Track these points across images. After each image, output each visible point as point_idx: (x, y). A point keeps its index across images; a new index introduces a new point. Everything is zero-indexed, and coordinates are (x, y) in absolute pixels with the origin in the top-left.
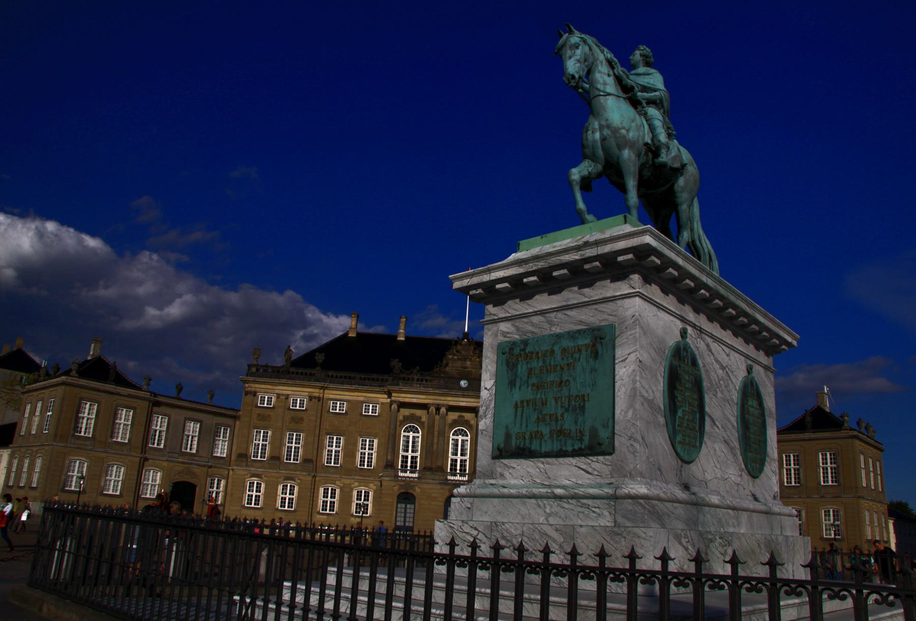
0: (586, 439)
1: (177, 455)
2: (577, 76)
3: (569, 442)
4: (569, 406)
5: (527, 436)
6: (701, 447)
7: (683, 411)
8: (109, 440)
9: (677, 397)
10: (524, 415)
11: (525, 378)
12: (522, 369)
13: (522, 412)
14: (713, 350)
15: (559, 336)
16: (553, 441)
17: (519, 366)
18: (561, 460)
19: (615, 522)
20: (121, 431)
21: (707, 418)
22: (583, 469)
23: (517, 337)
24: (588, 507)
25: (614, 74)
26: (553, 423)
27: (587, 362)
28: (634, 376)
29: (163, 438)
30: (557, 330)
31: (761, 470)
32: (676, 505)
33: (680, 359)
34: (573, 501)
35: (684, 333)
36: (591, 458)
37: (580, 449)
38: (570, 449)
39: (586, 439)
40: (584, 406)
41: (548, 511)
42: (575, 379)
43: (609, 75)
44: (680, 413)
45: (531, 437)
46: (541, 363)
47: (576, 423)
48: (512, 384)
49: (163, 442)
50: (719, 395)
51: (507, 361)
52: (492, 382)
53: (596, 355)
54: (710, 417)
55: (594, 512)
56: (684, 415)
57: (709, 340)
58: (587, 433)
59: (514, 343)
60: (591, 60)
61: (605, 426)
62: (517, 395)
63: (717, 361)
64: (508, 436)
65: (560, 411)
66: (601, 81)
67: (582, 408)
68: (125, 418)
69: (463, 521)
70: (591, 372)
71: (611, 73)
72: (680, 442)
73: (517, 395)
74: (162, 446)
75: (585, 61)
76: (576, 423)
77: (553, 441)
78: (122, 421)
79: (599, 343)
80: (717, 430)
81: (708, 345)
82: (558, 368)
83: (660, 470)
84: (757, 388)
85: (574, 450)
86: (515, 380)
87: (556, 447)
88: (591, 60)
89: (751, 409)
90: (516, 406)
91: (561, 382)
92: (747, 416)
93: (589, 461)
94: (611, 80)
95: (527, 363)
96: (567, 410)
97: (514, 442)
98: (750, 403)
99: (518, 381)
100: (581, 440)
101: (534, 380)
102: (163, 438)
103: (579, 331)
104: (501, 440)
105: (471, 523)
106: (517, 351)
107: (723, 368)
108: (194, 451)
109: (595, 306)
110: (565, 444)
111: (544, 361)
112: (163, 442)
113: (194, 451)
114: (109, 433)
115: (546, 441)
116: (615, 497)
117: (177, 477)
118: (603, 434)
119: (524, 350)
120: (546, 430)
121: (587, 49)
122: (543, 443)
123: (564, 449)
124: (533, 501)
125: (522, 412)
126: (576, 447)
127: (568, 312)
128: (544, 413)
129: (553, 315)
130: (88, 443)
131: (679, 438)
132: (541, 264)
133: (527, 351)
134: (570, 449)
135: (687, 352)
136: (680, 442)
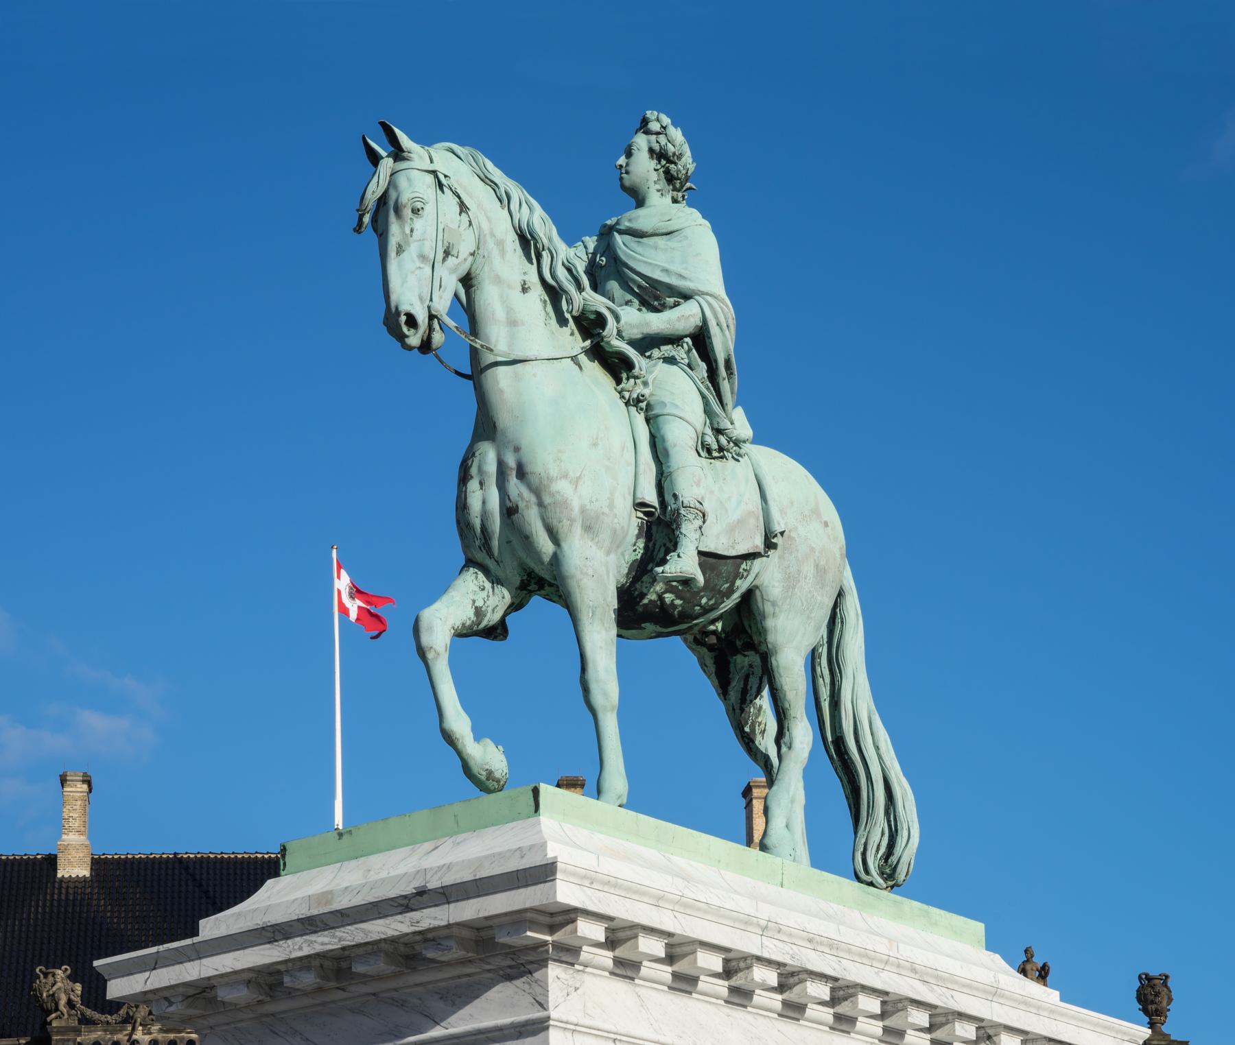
2: (422, 318)
43: (525, 290)
60: (465, 247)
71: (534, 278)
75: (447, 253)
88: (465, 247)
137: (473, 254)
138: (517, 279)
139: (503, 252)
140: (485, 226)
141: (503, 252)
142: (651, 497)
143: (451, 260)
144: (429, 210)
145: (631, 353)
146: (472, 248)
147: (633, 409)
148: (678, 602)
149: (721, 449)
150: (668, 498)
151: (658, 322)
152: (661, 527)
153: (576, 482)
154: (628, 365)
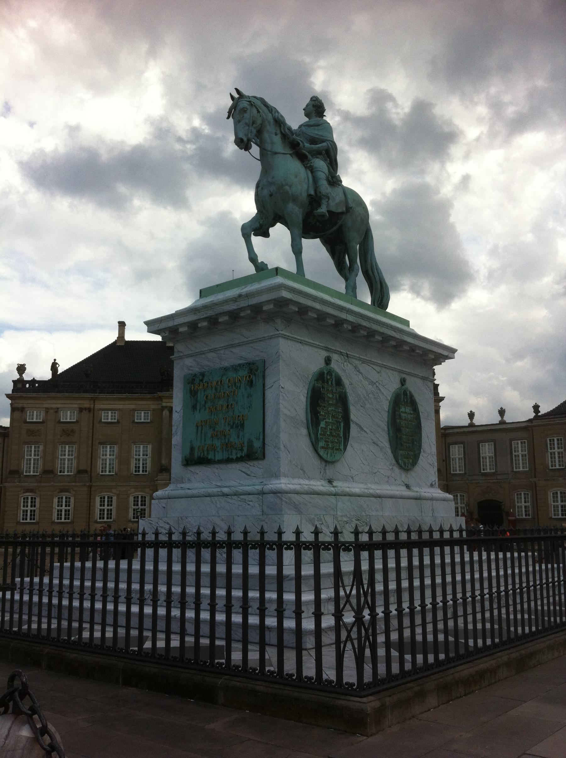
0: (245, 449)
2: (245, 139)
3: (234, 452)
4: (234, 423)
5: (206, 448)
6: (345, 449)
7: (326, 422)
9: (320, 413)
10: (203, 432)
11: (203, 403)
12: (201, 396)
13: (202, 430)
14: (362, 370)
15: (226, 369)
16: (223, 452)
17: (199, 393)
18: (229, 466)
19: (263, 511)
21: (352, 426)
22: (244, 472)
23: (198, 370)
24: (245, 501)
25: (281, 132)
26: (223, 437)
27: (246, 389)
28: (287, 397)
30: (225, 364)
31: (414, 463)
32: (312, 496)
33: (323, 381)
34: (235, 497)
35: (328, 361)
36: (249, 463)
37: (241, 456)
38: (234, 457)
39: (245, 449)
40: (244, 423)
41: (218, 505)
42: (237, 403)
43: (276, 134)
44: (323, 424)
45: (208, 450)
46: (214, 391)
47: (238, 437)
48: (194, 407)
50: (368, 406)
51: (190, 389)
52: (181, 406)
53: (251, 384)
54: (357, 424)
55: (249, 504)
56: (327, 426)
57: (357, 362)
58: (246, 444)
59: (195, 375)
60: (259, 121)
61: (258, 439)
62: (199, 416)
63: (366, 378)
64: (192, 449)
65: (227, 428)
66: (268, 140)
67: (242, 425)
69: (159, 518)
70: (248, 397)
71: (278, 132)
72: (322, 447)
73: (199, 416)
75: (253, 123)
76: (238, 437)
77: (223, 452)
79: (255, 374)
80: (365, 434)
81: (356, 367)
82: (226, 394)
83: (302, 470)
84: (412, 396)
85: (237, 458)
86: (196, 405)
87: (226, 456)
89: (403, 415)
90: (197, 426)
91: (228, 406)
92: (398, 421)
93: (248, 466)
94: (278, 139)
95: (205, 391)
96: (232, 427)
97: (196, 454)
98: (403, 409)
99: (198, 405)
100: (242, 450)
101: (209, 405)
103: (239, 365)
104: (188, 451)
105: (165, 519)
106: (197, 381)
107: (372, 383)
109: (251, 345)
110: (231, 454)
111: (216, 389)
115: (218, 452)
116: (262, 493)
118: (257, 445)
119: (202, 380)
120: (217, 443)
121: (255, 111)
122: (216, 453)
123: (230, 457)
124: (208, 498)
125: (202, 430)
126: (239, 456)
127: (233, 350)
128: (216, 429)
129: (222, 352)
131: (321, 444)
132: (210, 313)
133: (204, 381)
134: (234, 457)
135: (331, 375)
136: (322, 447)
137: (261, 124)
138: (274, 131)
139: (270, 125)
140: (265, 117)
141: (270, 125)
142: (312, 192)
143: (254, 125)
144: (248, 111)
145: (307, 154)
146: (261, 122)
147: (308, 170)
148: (321, 225)
149: (334, 182)
150: (318, 193)
151: (314, 147)
152: (315, 200)
153: (290, 187)
154: (306, 157)
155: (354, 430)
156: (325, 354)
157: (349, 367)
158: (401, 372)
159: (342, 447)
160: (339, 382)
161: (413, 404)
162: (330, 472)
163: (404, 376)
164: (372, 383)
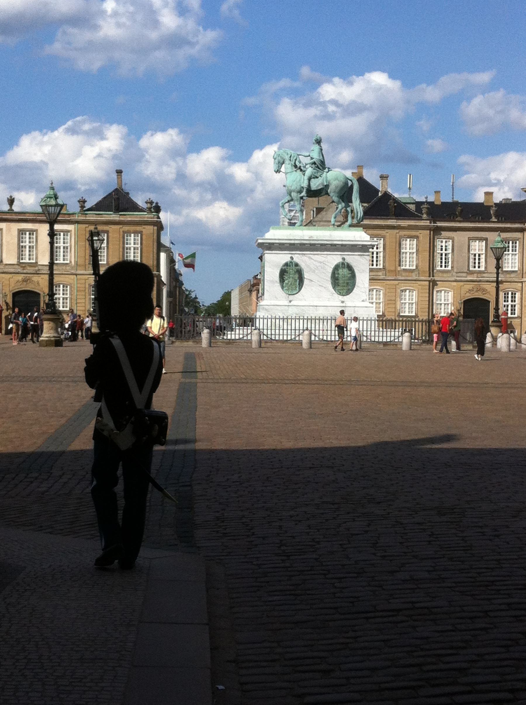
1: (464, 275)
6: (300, 289)
8: (399, 268)
20: (408, 260)
29: (450, 260)
44: (286, 282)
49: (450, 263)
50: (316, 271)
63: (315, 261)
68: (409, 247)
74: (449, 268)
78: (408, 250)
92: (337, 276)
102: (450, 260)
108: (482, 269)
112: (450, 263)
113: (482, 269)
114: (397, 263)
117: (468, 294)
130: (380, 274)
131: (285, 289)
155: (306, 282)
156: (290, 255)
157: (305, 258)
158: (341, 255)
159: (298, 289)
160: (297, 265)
161: (350, 268)
162: (291, 297)
163: (344, 256)
164: (321, 262)
